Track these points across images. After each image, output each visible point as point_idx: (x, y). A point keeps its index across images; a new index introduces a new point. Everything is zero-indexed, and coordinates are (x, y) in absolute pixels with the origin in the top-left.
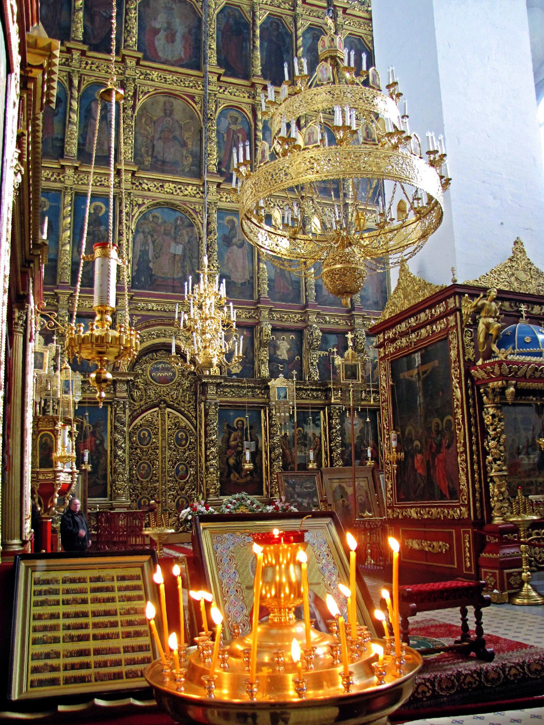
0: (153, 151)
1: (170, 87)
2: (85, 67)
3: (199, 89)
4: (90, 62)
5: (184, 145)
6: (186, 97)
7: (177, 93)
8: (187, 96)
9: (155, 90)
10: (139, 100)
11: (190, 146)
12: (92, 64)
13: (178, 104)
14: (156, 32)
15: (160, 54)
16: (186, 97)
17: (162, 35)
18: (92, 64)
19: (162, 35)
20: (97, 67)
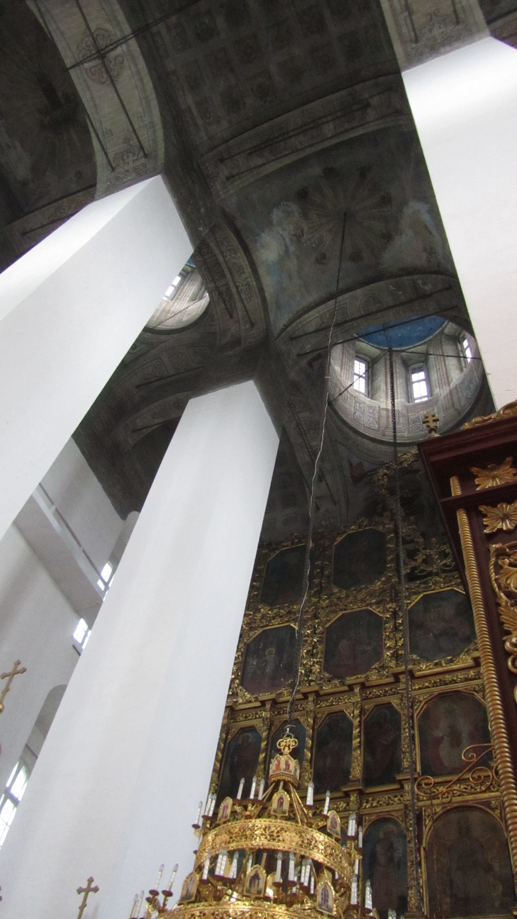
0: (452, 888)
1: (460, 799)
2: (366, 806)
3: (496, 789)
4: (370, 799)
5: (489, 869)
6: (480, 806)
7: (470, 804)
8: (479, 803)
9: (443, 808)
10: (426, 826)
11: (497, 869)
12: (373, 800)
13: (475, 817)
14: (439, 741)
15: (446, 764)
16: (480, 806)
17: (446, 743)
18: (373, 800)
19: (446, 743)
20: (378, 802)
